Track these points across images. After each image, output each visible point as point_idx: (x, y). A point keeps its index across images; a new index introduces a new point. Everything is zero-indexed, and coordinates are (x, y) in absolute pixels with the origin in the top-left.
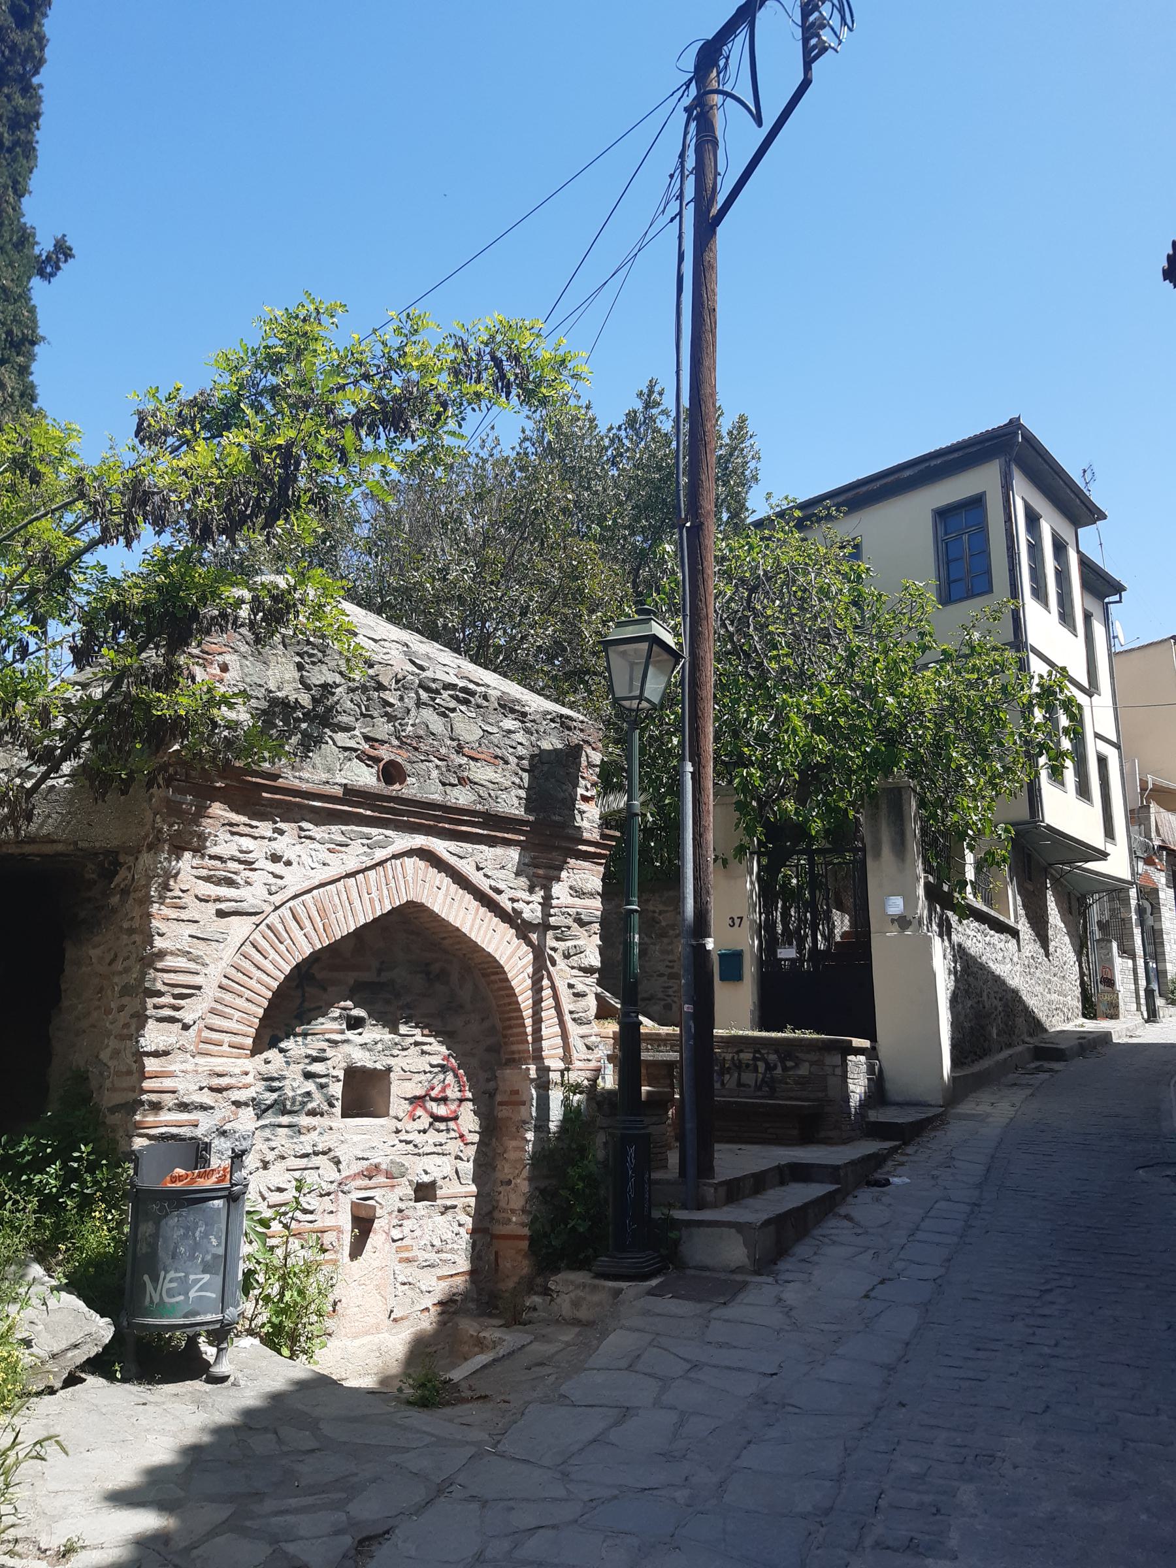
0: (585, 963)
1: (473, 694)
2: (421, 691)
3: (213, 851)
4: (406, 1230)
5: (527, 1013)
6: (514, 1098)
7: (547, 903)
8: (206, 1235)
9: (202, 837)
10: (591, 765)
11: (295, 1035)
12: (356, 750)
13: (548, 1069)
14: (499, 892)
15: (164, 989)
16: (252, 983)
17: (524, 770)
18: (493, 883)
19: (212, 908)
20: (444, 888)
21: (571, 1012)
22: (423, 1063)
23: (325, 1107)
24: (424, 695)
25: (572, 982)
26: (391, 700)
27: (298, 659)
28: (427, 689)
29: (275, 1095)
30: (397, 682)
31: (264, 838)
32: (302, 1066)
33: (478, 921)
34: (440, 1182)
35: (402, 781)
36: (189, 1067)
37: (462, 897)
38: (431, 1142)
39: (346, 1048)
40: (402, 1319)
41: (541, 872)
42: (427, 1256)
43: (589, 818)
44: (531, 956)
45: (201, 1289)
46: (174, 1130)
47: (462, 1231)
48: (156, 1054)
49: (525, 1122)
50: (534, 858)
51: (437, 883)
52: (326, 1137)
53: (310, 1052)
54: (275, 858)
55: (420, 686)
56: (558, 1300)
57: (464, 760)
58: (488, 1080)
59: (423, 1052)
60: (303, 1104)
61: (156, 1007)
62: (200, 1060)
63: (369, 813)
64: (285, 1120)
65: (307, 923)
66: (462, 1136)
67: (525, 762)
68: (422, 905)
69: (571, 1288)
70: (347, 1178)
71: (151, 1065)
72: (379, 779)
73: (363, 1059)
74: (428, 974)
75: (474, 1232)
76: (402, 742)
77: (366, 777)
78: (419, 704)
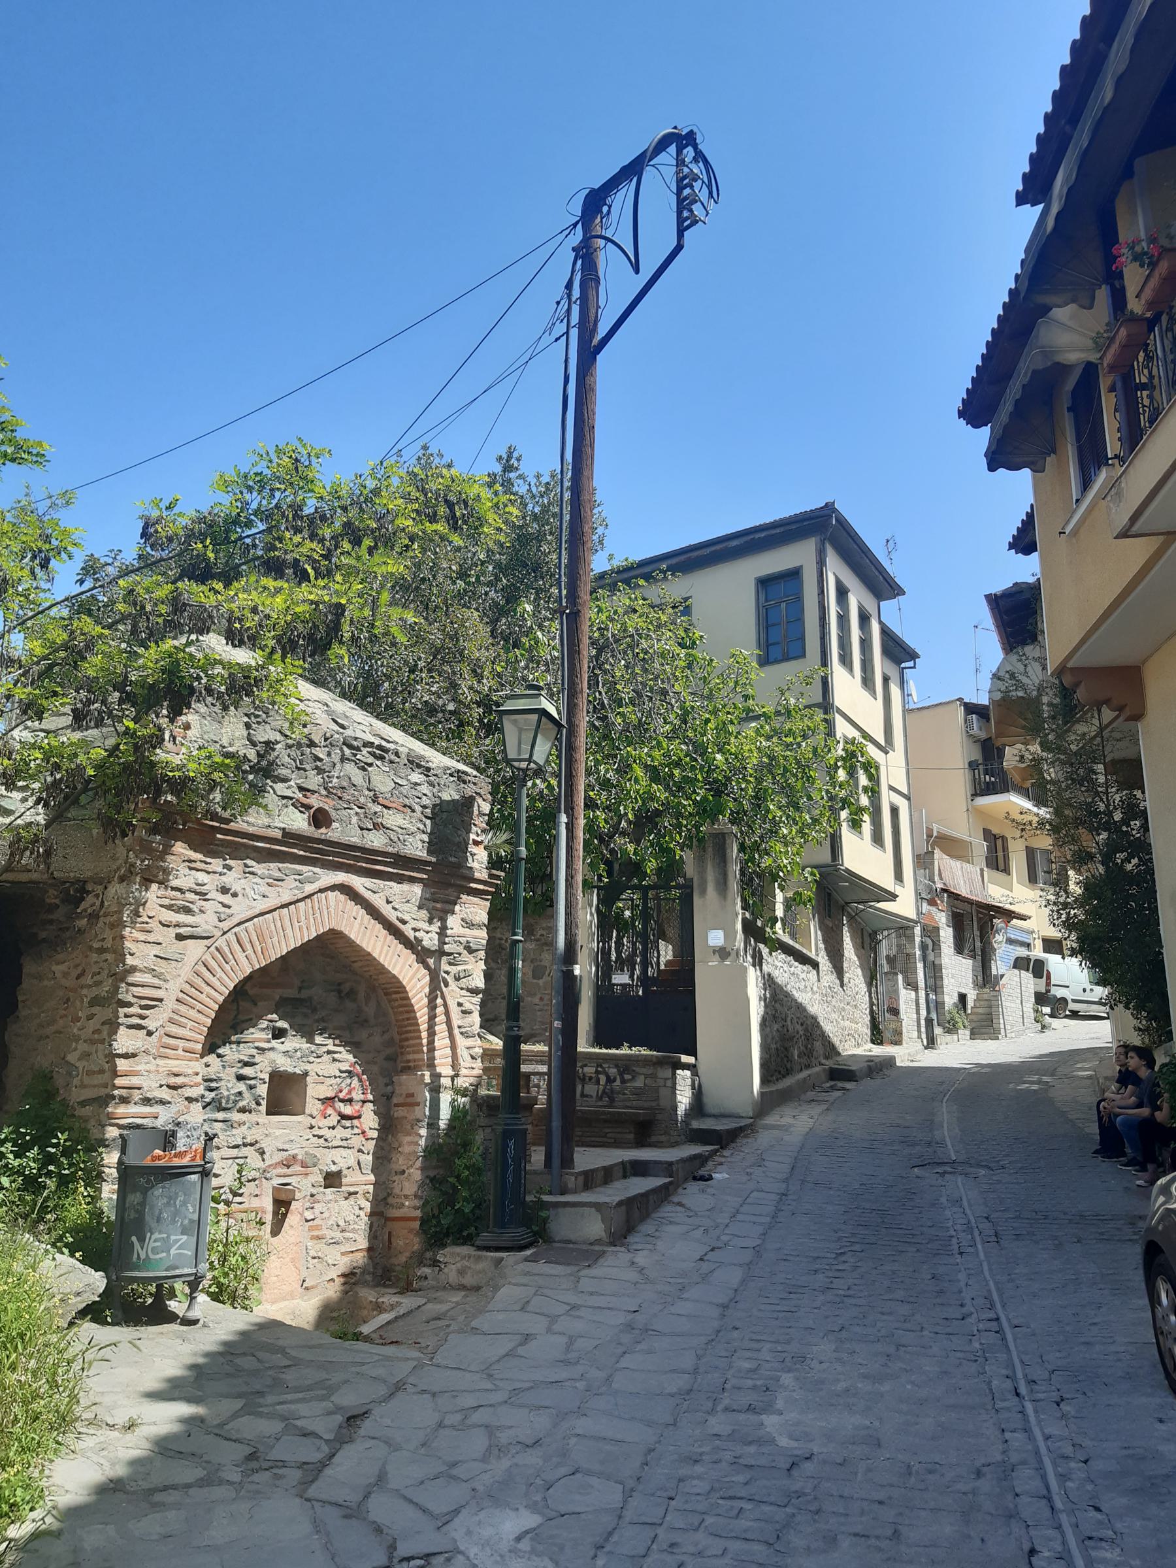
0: (472, 985)
1: (386, 751)
2: (345, 748)
3: (175, 883)
4: (317, 1212)
5: (424, 1027)
6: (409, 1100)
7: (442, 933)
8: (184, 1203)
9: (167, 872)
10: (481, 814)
11: (230, 1043)
12: (291, 798)
13: (439, 1076)
14: (404, 922)
15: (133, 1000)
16: (203, 997)
17: (427, 817)
18: (400, 915)
19: (173, 932)
20: (359, 918)
21: (459, 1027)
22: (333, 1069)
23: (254, 1106)
24: (347, 751)
25: (461, 1001)
26: (321, 756)
27: (246, 719)
28: (350, 747)
29: (213, 1094)
30: (326, 739)
31: (215, 873)
32: (235, 1070)
33: (386, 947)
34: (345, 1172)
35: (328, 826)
36: (152, 1067)
37: (374, 926)
38: (338, 1137)
39: (271, 1055)
40: (312, 1288)
41: (438, 906)
42: (333, 1234)
43: (478, 860)
44: (428, 978)
45: (179, 1248)
46: (139, 1121)
47: (362, 1213)
48: (126, 1056)
49: (419, 1121)
50: (434, 894)
51: (354, 914)
52: (253, 1131)
53: (242, 1057)
54: (224, 890)
55: (344, 744)
56: (446, 1270)
57: (378, 808)
58: (387, 1085)
59: (334, 1060)
60: (236, 1102)
61: (126, 1016)
62: (161, 1062)
63: (301, 853)
64: (220, 1115)
65: (248, 946)
66: (363, 1133)
67: (428, 811)
68: (341, 933)
69: (457, 1260)
70: (270, 1166)
71: (122, 1065)
72: (309, 824)
73: (286, 1065)
74: (340, 992)
75: (372, 1215)
76: (329, 792)
77: (299, 822)
78: (343, 759)
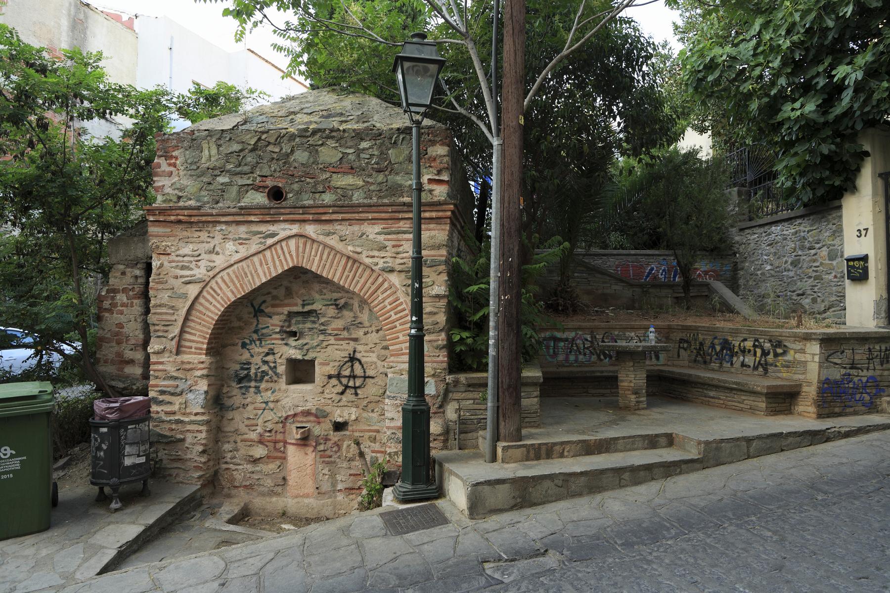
15: (158, 323)
29: (246, 372)
73: (297, 355)
74: (337, 305)
